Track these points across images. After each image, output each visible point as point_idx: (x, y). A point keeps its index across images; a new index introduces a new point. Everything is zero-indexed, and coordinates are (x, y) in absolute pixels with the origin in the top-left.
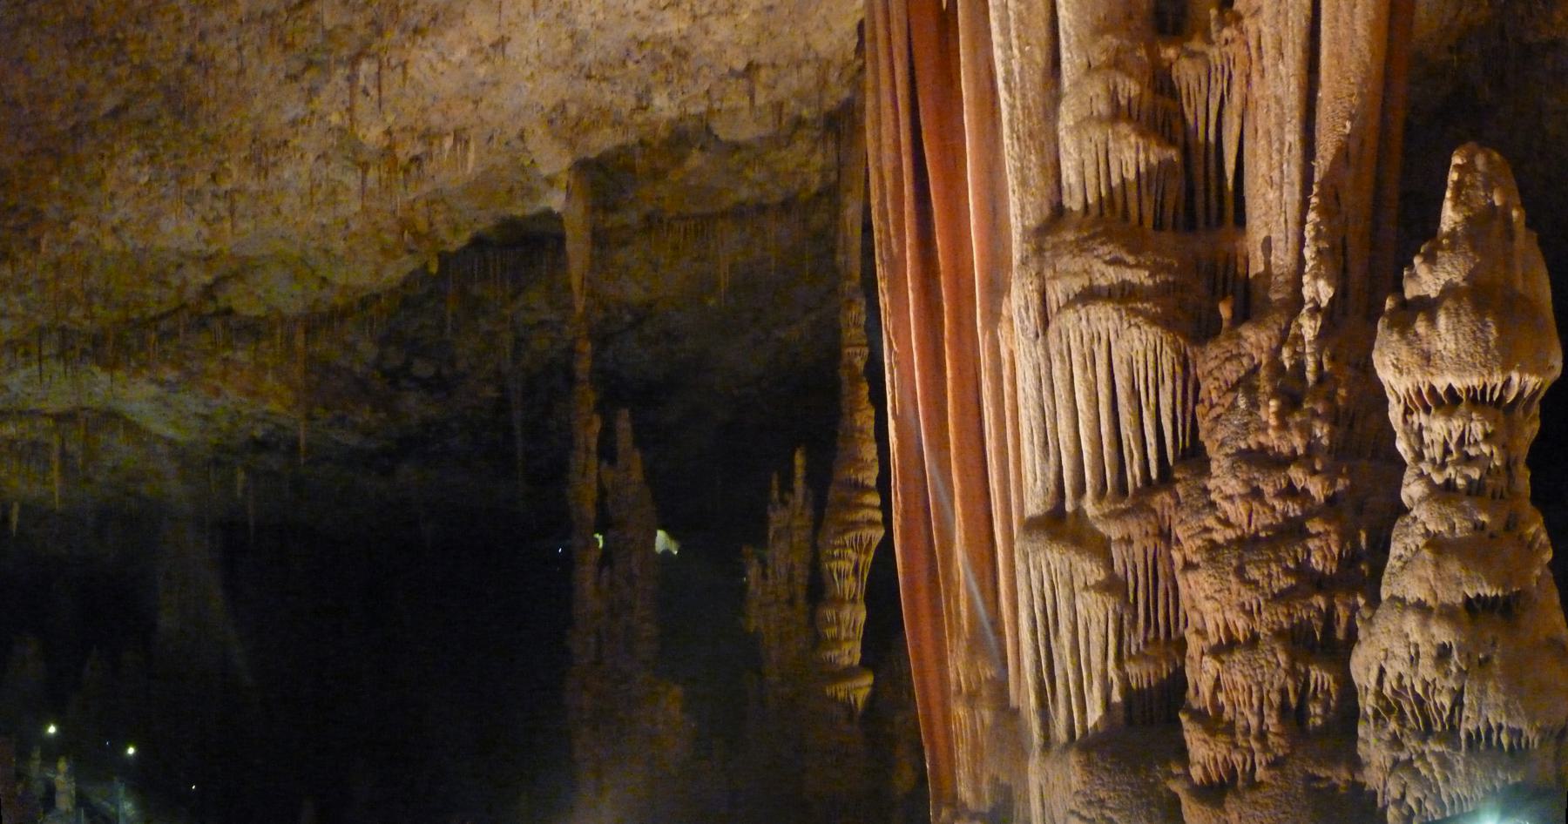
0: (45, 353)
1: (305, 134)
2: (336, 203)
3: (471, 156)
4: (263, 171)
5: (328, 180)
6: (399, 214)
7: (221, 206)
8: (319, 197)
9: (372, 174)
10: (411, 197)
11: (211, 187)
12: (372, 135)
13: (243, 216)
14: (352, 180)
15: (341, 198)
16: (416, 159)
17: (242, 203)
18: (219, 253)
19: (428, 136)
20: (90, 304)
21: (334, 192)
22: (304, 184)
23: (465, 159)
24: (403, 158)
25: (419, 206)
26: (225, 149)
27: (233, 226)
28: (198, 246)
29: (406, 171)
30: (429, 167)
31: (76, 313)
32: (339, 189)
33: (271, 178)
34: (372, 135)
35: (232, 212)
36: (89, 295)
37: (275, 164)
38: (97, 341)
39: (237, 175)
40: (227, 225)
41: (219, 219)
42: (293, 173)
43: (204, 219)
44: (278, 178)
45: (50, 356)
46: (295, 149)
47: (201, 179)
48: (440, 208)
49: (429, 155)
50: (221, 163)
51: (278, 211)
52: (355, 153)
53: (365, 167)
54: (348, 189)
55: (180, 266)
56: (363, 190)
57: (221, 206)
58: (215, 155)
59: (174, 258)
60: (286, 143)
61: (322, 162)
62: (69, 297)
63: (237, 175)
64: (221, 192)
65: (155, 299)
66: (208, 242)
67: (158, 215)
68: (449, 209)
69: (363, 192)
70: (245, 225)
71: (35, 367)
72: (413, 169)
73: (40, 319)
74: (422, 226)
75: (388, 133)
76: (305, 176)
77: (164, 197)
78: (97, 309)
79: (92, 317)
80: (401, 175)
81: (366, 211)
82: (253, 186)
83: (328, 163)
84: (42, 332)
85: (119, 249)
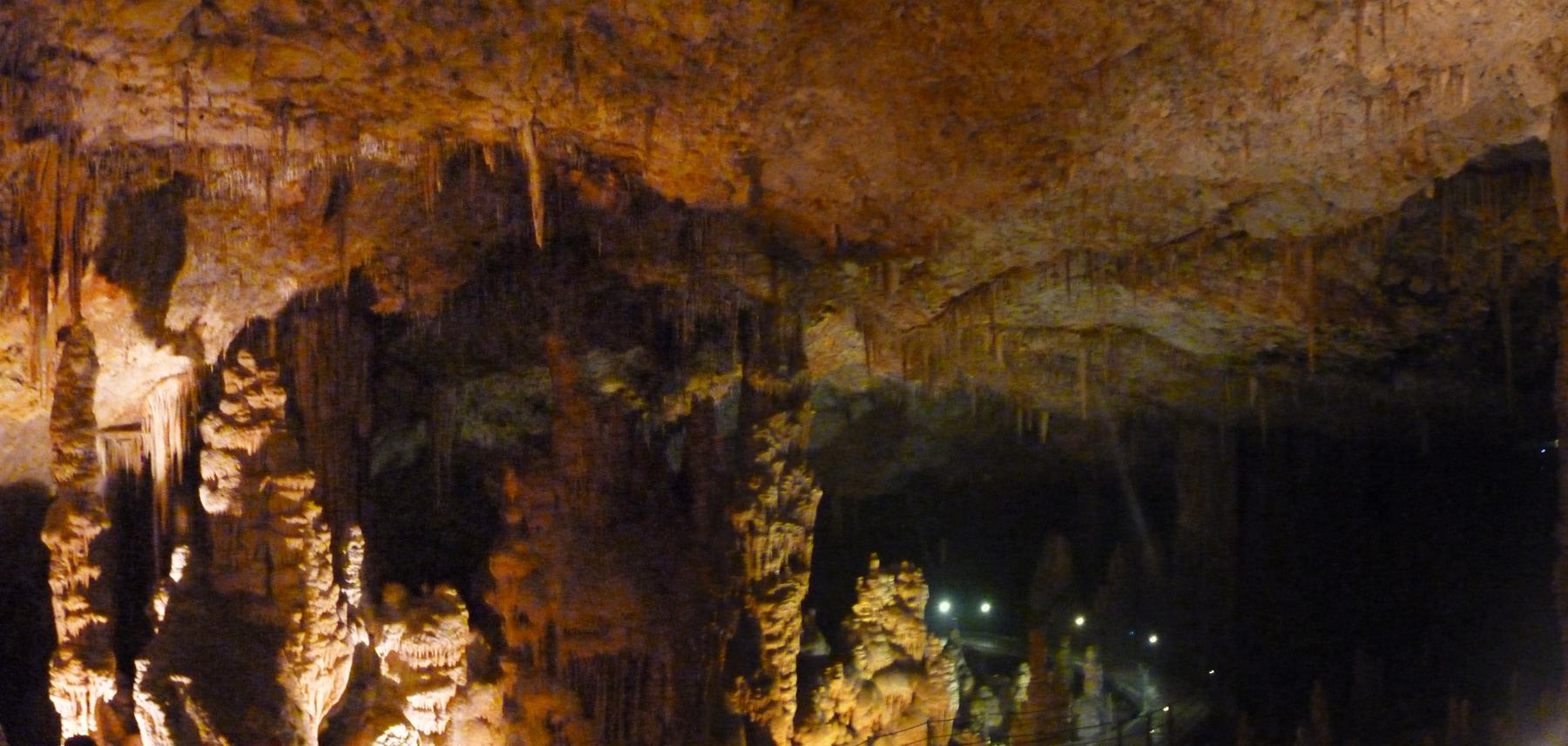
0: (1073, 274)
1: (1314, 70)
2: (1340, 134)
3: (1466, 91)
4: (1276, 105)
5: (1335, 114)
6: (1399, 145)
7: (1237, 138)
8: (1327, 126)
9: (1376, 107)
10: (1411, 127)
11: (1229, 120)
12: (1375, 71)
13: (1257, 147)
14: (1356, 112)
15: (1346, 130)
16: (1414, 94)
17: (1255, 132)
18: (1233, 180)
19: (1425, 71)
20: (1115, 228)
21: (1339, 124)
22: (1313, 116)
23: (1460, 94)
24: (1403, 94)
25: (1418, 136)
26: (1240, 84)
27: (1248, 156)
28: (1214, 175)
29: (1406, 103)
30: (1427, 101)
31: (1102, 237)
32: (1345, 122)
33: (1283, 111)
34: (1375, 71)
35: (1247, 144)
36: (1114, 220)
37: (1286, 98)
38: (1121, 262)
39: (1251, 109)
40: (1243, 154)
41: (1234, 149)
42: (1305, 106)
43: (1220, 149)
44: (1289, 111)
45: (1078, 276)
46: (1305, 84)
47: (1217, 113)
48: (1435, 138)
49: (1427, 89)
50: (1236, 97)
51: (1288, 142)
52: (1359, 88)
53: (1368, 100)
54: (1353, 121)
55: (1198, 193)
56: (1367, 120)
57: (1237, 138)
58: (1231, 90)
59: (1192, 186)
60: (1296, 78)
61: (1329, 97)
62: (1095, 224)
63: (1251, 109)
64: (1236, 125)
65: (1175, 223)
66: (1224, 171)
67: (1174, 149)
68: (1444, 139)
69: (1368, 125)
70: (1258, 154)
71: (1063, 287)
72: (1413, 103)
73: (1068, 243)
74: (1420, 155)
75: (1390, 69)
76: (1313, 110)
77: (1184, 129)
78: (1122, 235)
79: (1115, 240)
80: (1402, 110)
81: (1369, 143)
82: (1266, 118)
83: (1335, 98)
84: (1069, 255)
85: (1142, 178)
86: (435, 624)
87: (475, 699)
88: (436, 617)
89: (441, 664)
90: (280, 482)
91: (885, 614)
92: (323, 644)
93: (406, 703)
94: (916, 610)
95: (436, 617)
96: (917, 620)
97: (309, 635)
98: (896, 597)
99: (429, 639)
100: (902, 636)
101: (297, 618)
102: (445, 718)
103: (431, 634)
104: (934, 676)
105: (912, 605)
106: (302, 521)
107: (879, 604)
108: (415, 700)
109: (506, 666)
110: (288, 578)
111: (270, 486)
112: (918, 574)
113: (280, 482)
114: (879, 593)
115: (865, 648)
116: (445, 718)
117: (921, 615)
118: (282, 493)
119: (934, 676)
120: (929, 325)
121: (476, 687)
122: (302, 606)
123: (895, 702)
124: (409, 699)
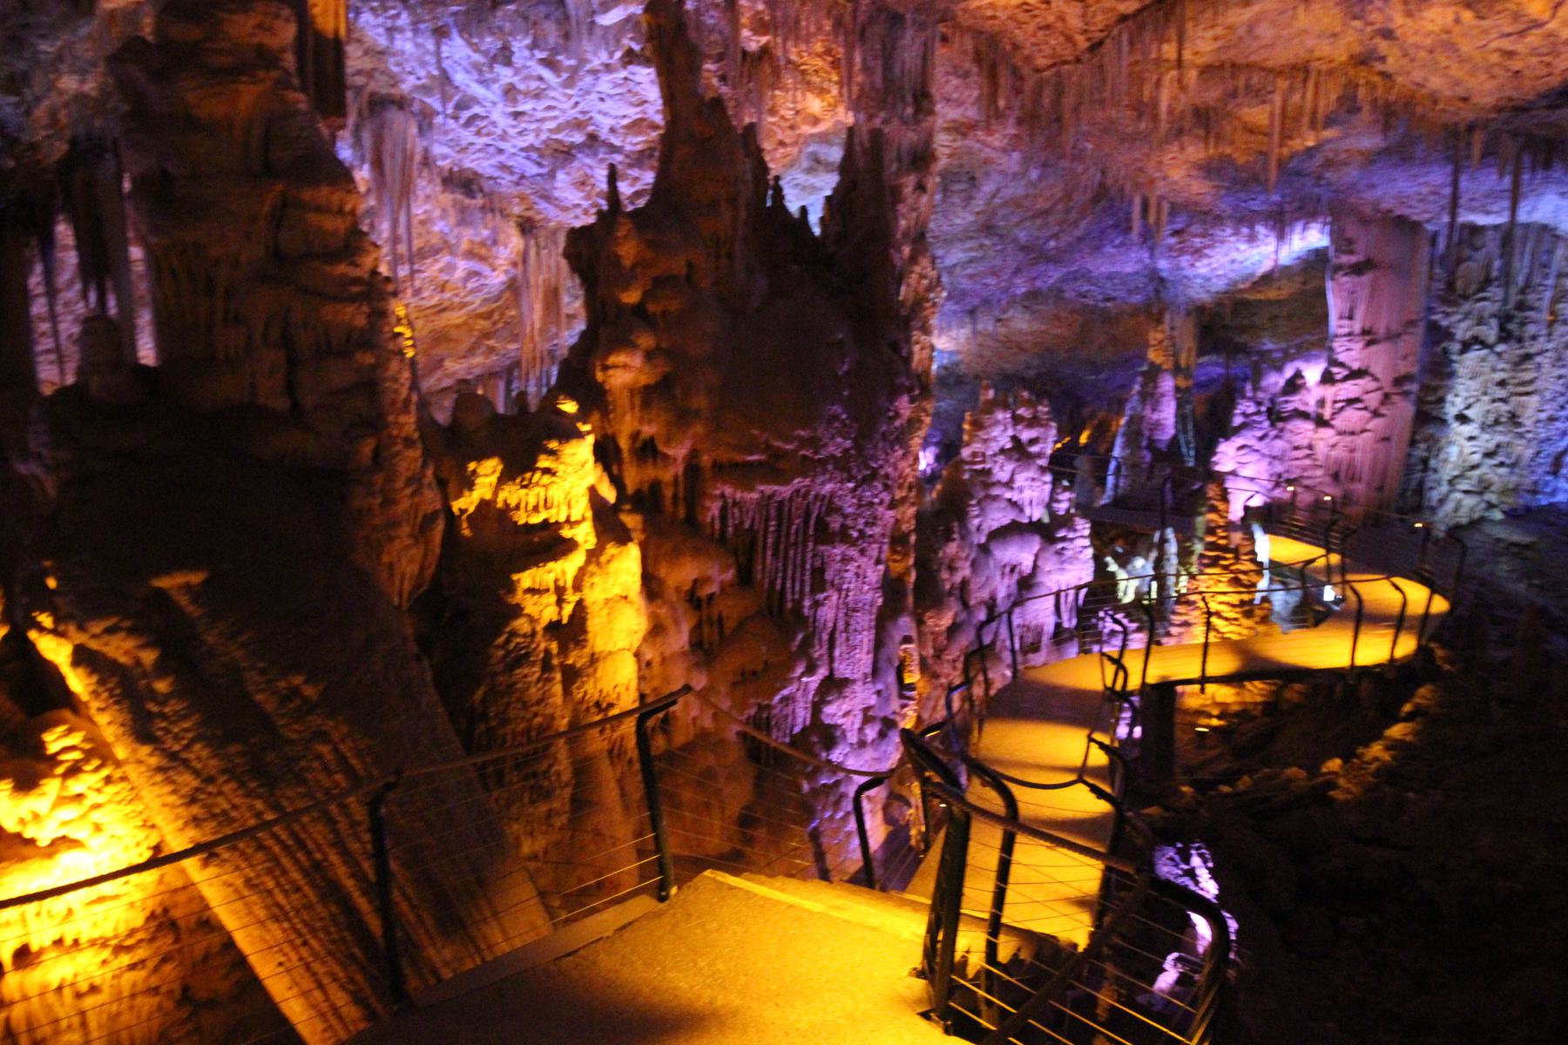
86: (553, 453)
87: (613, 566)
88: (553, 445)
89: (562, 519)
90: (307, 195)
91: (1000, 459)
92: (408, 491)
93: (511, 587)
94: (1039, 455)
95: (553, 445)
96: (1043, 470)
97: (391, 477)
98: (1015, 439)
99: (546, 479)
100: (1021, 490)
101: (367, 448)
102: (572, 598)
103: (547, 471)
104: (1064, 539)
105: (1034, 449)
106: (354, 272)
107: (994, 447)
108: (526, 579)
109: (631, 520)
110: (338, 375)
111: (284, 204)
112: (1043, 409)
113: (307, 195)
114: (996, 432)
115: (979, 503)
116: (572, 598)
117: (1043, 462)
118: (313, 218)
119: (1064, 539)
120: (1078, 60)
121: (611, 549)
122: (375, 424)
123: (1012, 570)
124: (515, 577)
